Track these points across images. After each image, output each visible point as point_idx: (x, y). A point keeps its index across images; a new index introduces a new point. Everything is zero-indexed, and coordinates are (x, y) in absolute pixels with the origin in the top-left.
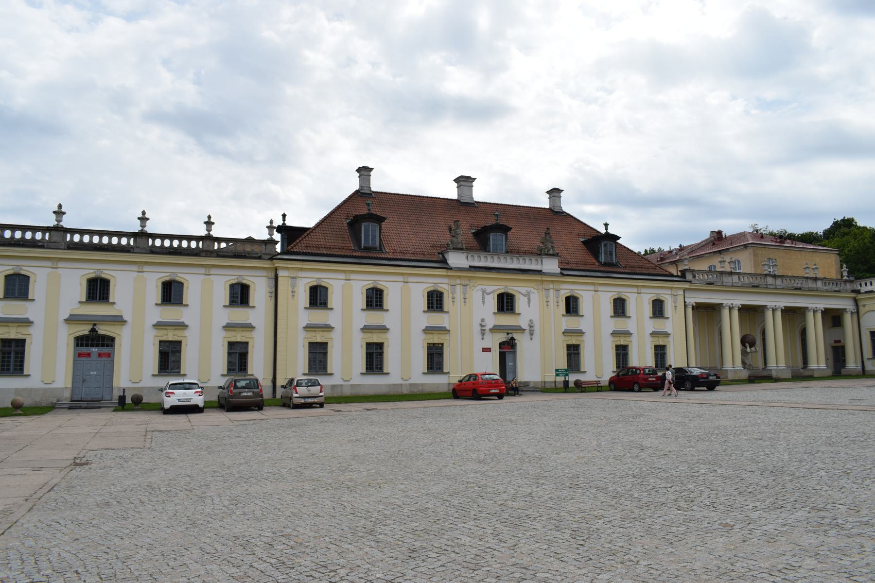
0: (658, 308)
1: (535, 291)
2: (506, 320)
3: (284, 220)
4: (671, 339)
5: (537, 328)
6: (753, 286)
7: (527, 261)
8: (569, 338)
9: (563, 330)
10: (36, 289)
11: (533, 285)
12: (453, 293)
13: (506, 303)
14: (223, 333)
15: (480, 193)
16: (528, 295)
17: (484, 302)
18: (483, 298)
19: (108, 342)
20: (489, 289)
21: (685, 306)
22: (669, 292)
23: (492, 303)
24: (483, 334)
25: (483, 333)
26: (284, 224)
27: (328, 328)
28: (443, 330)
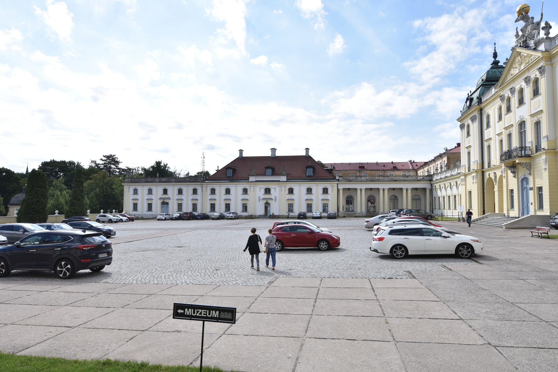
0: (325, 191)
1: (278, 187)
2: (267, 196)
3: (218, 168)
4: (330, 201)
5: (278, 199)
6: (371, 181)
7: (275, 178)
8: (289, 201)
9: (287, 199)
10: (154, 192)
11: (276, 185)
12: (250, 189)
13: (268, 191)
14: (191, 201)
15: (278, 154)
16: (275, 188)
17: (260, 191)
18: (260, 190)
19: (167, 204)
20: (262, 187)
21: (338, 190)
22: (330, 185)
23: (263, 191)
24: (259, 201)
25: (259, 200)
26: (218, 169)
27: (215, 199)
28: (247, 200)
